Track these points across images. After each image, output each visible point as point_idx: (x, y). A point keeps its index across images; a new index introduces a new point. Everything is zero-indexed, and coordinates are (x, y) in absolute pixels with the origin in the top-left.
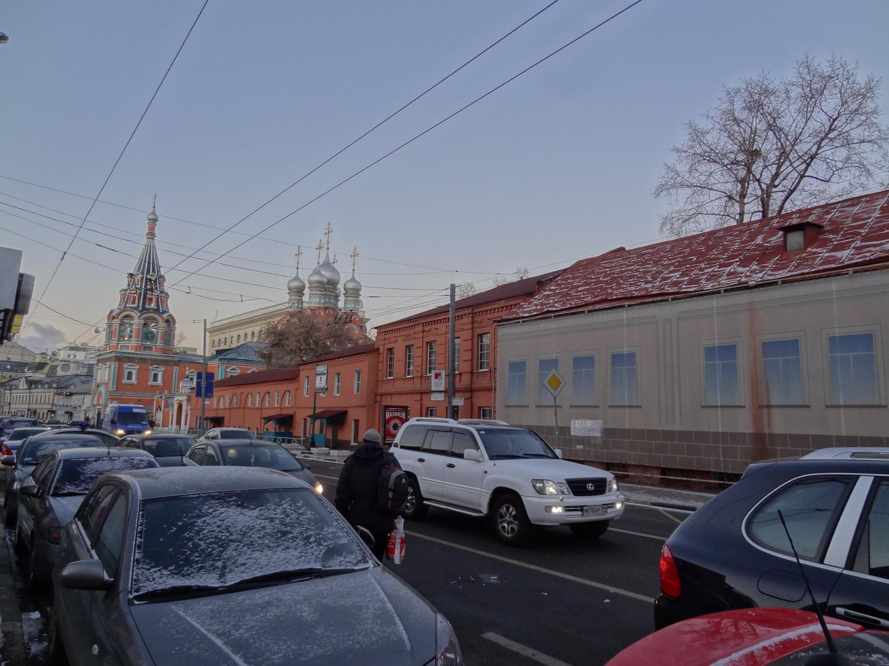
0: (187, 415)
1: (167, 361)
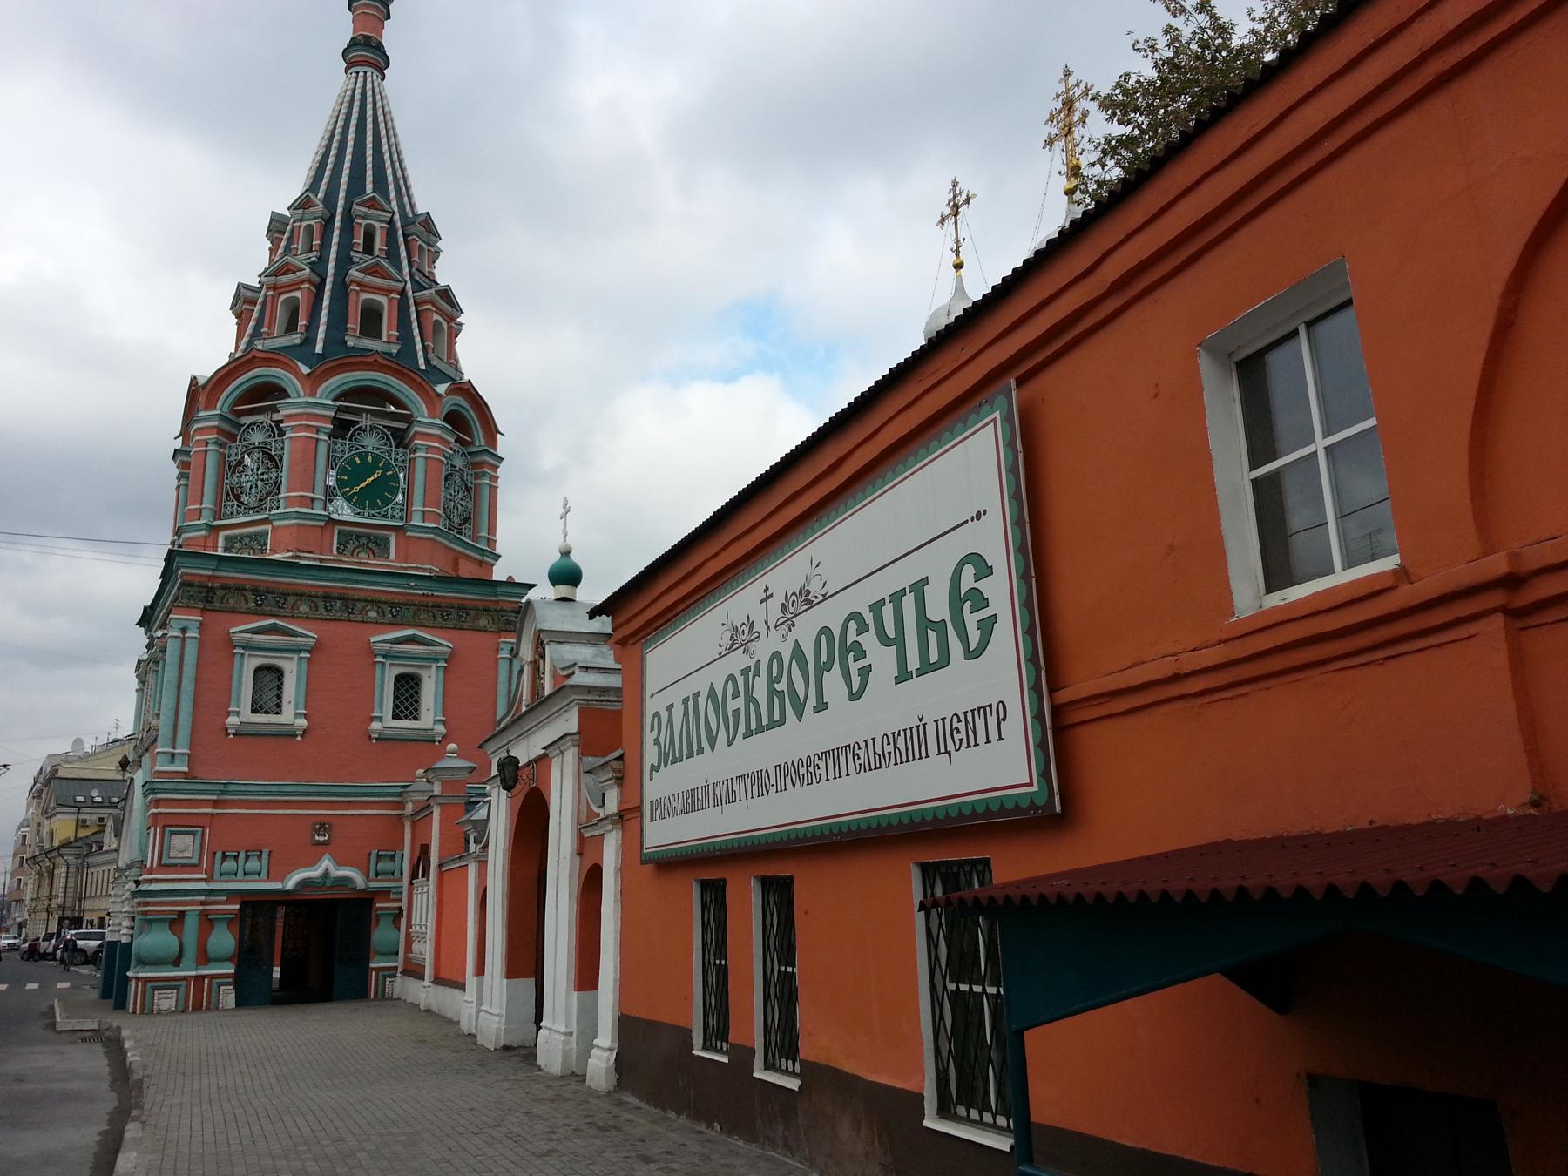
0: (591, 882)
1: (462, 609)
